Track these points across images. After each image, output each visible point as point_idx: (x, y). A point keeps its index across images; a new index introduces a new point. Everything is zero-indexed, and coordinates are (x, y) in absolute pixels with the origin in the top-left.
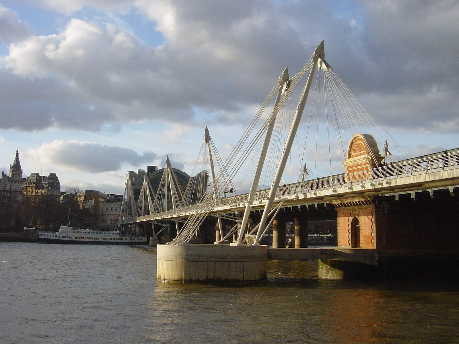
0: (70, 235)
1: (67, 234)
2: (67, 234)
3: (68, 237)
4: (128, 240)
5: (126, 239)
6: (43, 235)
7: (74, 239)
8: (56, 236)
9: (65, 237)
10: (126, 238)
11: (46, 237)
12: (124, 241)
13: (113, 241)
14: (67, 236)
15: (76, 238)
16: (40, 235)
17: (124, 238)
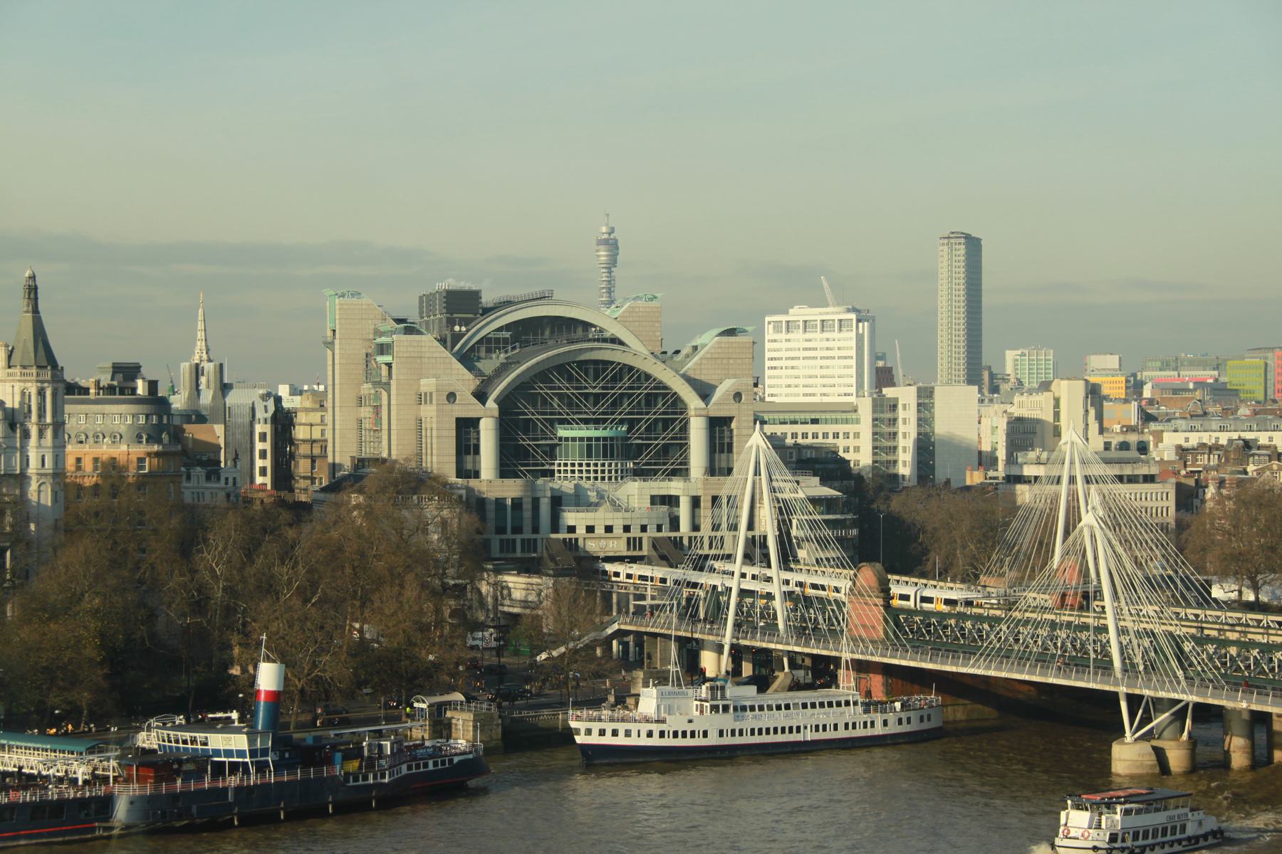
0: (698, 727)
1: (690, 721)
2: (690, 721)
3: (693, 734)
4: (893, 728)
5: (885, 723)
6: (589, 729)
7: (713, 740)
8: (650, 734)
9: (684, 734)
10: (885, 716)
11: (608, 740)
12: (879, 730)
13: (842, 733)
14: (689, 728)
15: (721, 733)
16: (583, 732)
17: (879, 718)
